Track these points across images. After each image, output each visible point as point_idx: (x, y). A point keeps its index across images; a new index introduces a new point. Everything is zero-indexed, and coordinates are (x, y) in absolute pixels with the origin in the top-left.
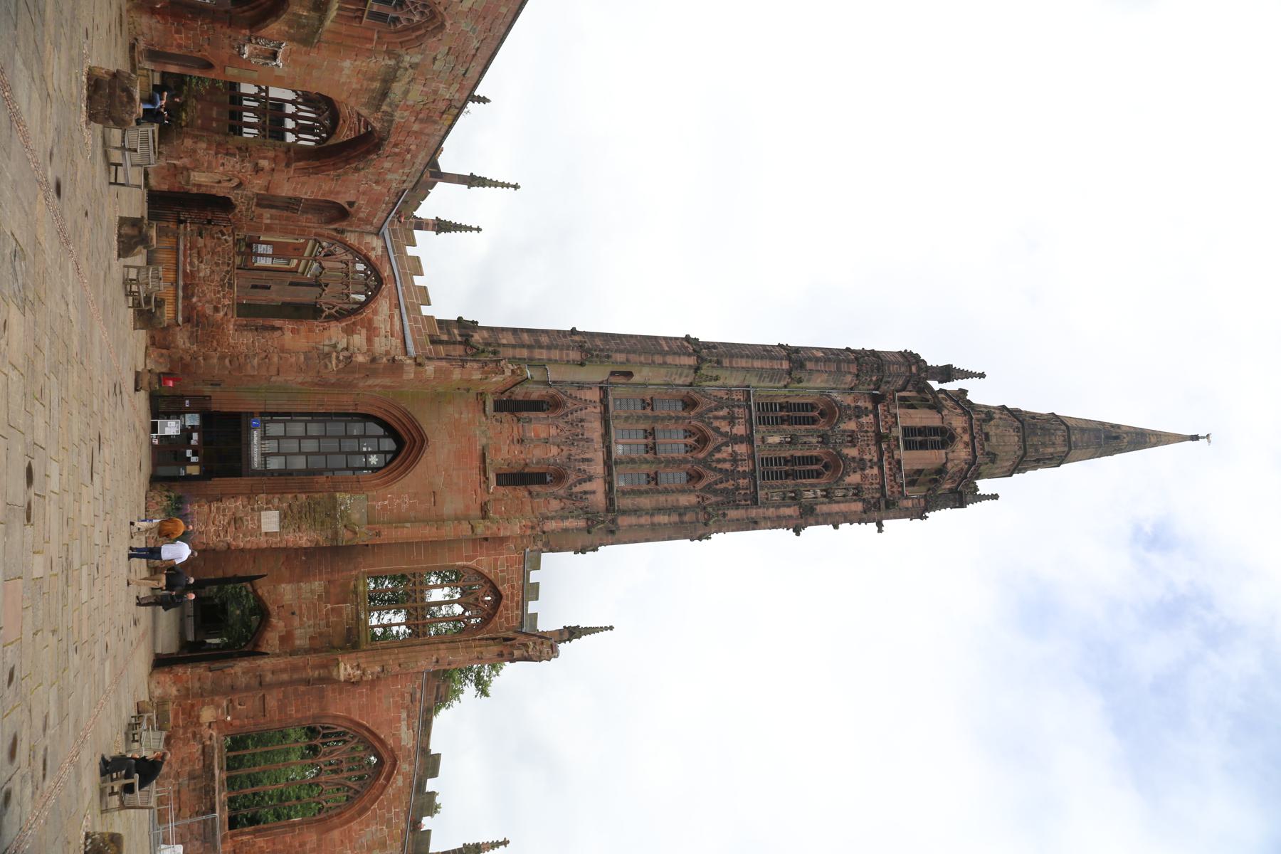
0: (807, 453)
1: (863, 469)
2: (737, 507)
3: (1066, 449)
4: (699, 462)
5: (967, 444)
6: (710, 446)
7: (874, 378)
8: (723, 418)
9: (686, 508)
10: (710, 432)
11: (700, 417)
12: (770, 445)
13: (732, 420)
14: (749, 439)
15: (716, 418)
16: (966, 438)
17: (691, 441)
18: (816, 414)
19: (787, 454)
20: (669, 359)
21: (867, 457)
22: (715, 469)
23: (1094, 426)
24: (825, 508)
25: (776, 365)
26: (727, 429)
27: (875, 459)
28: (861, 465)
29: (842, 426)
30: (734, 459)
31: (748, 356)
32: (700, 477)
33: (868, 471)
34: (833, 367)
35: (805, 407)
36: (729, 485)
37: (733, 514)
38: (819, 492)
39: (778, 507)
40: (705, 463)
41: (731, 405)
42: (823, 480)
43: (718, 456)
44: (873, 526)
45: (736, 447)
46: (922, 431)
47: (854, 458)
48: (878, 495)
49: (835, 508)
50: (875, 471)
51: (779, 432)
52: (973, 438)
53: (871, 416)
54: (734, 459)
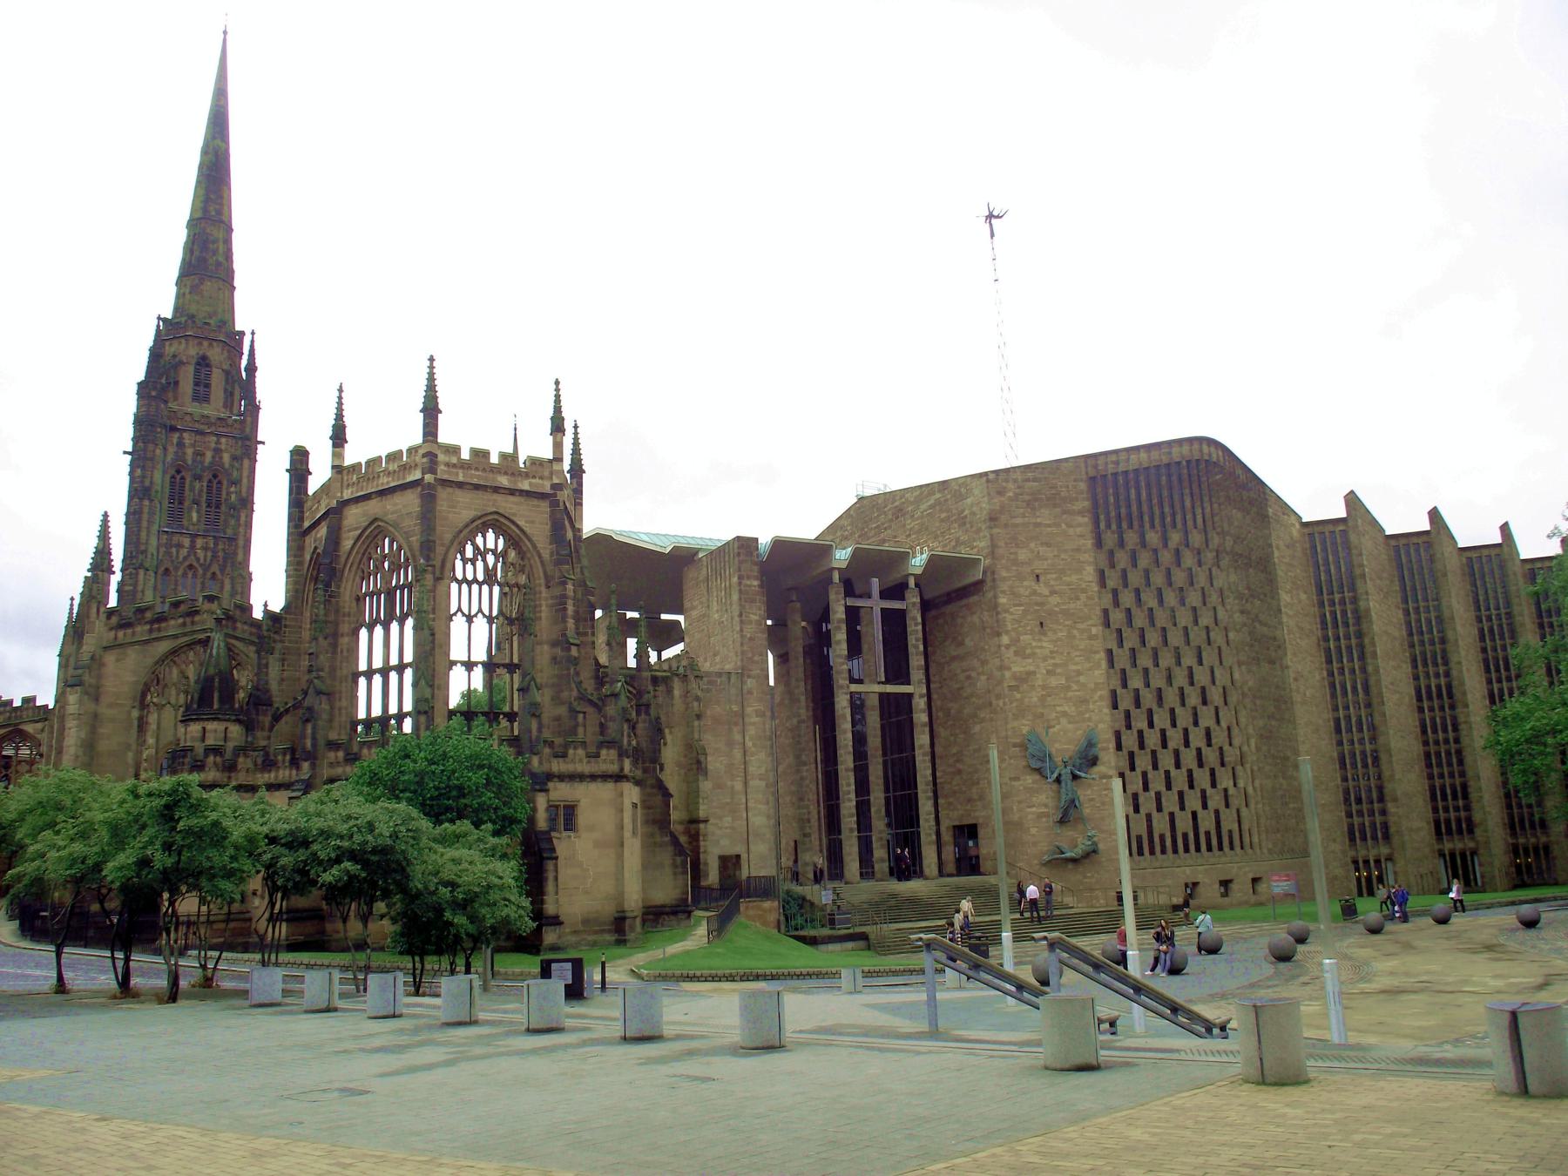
0: (205, 490)
1: (221, 450)
2: (235, 554)
3: (222, 225)
4: (204, 574)
5: (211, 345)
6: (195, 564)
7: (159, 430)
8: (178, 552)
9: (233, 588)
10: (187, 563)
11: (177, 569)
12: (199, 521)
13: (179, 546)
14: (194, 537)
15: (177, 557)
16: (206, 343)
17: (190, 575)
18: (178, 477)
19: (204, 505)
20: (140, 588)
21: (213, 445)
22: (210, 565)
23: (202, 192)
24: (244, 490)
25: (146, 510)
26: (186, 550)
27: (215, 438)
28: (217, 451)
29: (190, 462)
30: (205, 549)
31: (139, 531)
32: (214, 573)
33: (223, 447)
34: (149, 464)
35: (172, 484)
36: (221, 554)
37: (240, 557)
38: (233, 489)
39: (239, 525)
40: (206, 569)
41: (169, 545)
42: (225, 483)
43: (202, 561)
44: (259, 446)
45: (198, 546)
46: (197, 384)
47: (213, 457)
48: (240, 443)
49: (245, 481)
50: (223, 440)
51: (190, 509)
52: (206, 338)
53: (185, 435)
54: (205, 549)
